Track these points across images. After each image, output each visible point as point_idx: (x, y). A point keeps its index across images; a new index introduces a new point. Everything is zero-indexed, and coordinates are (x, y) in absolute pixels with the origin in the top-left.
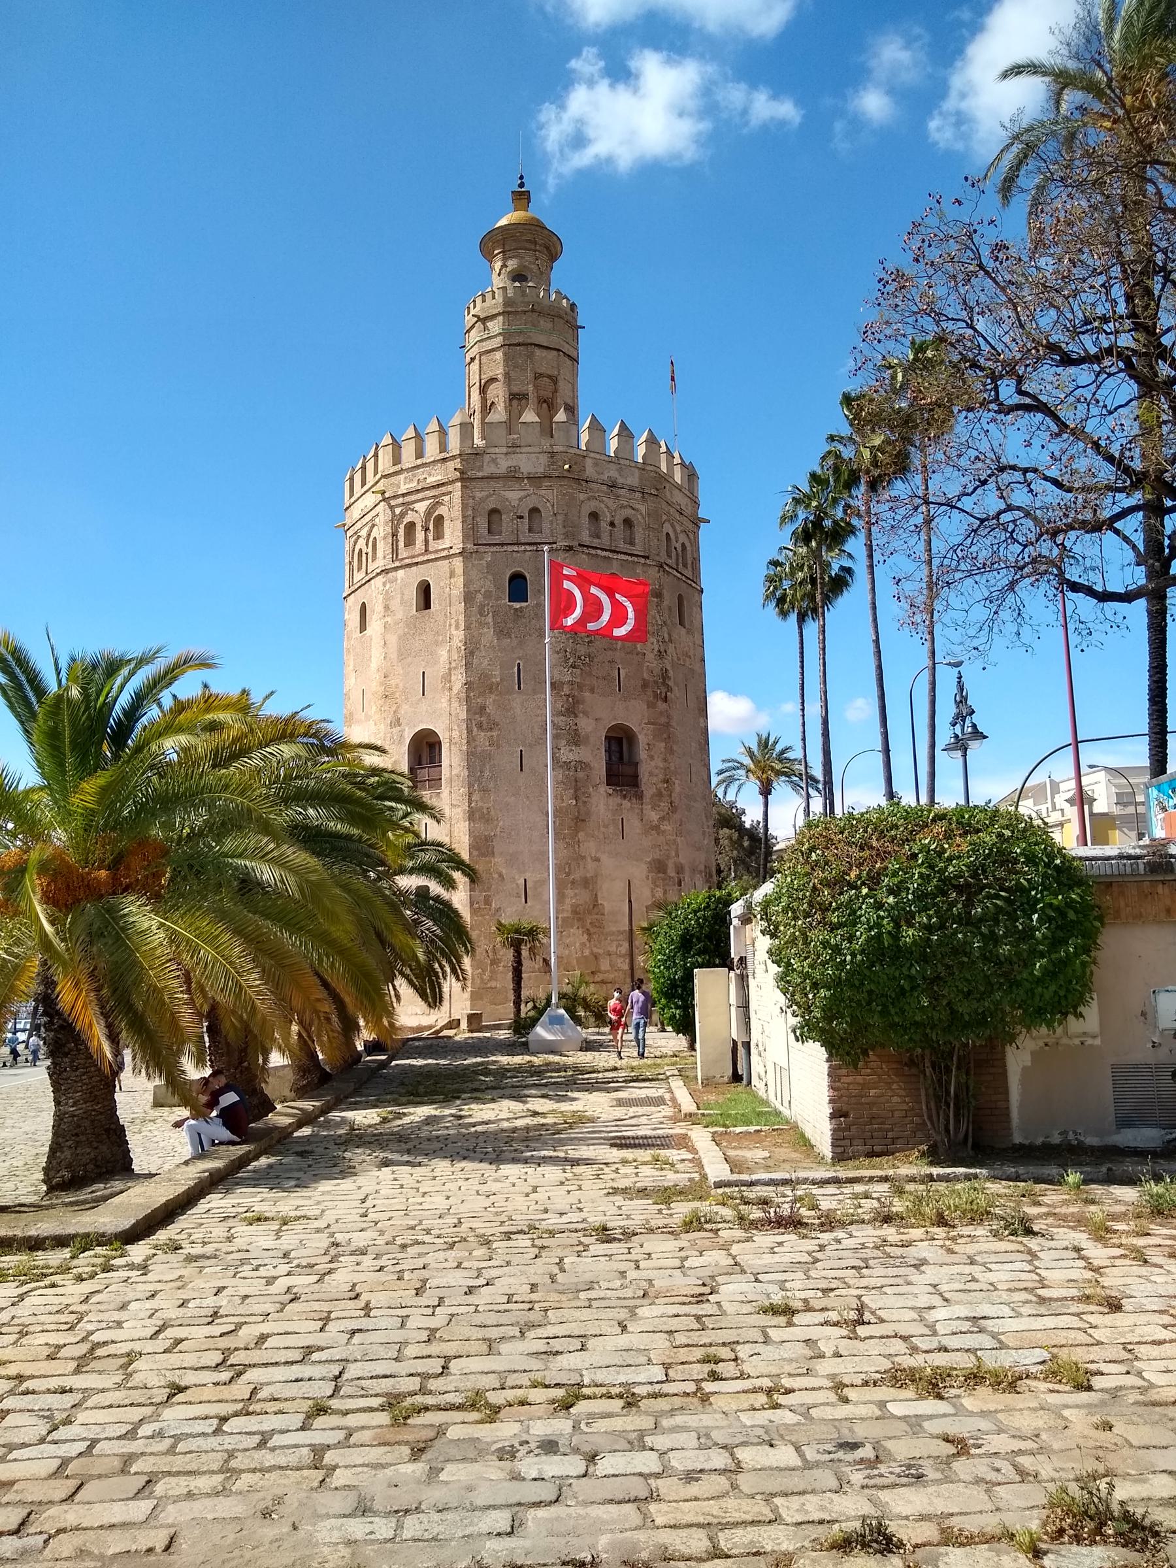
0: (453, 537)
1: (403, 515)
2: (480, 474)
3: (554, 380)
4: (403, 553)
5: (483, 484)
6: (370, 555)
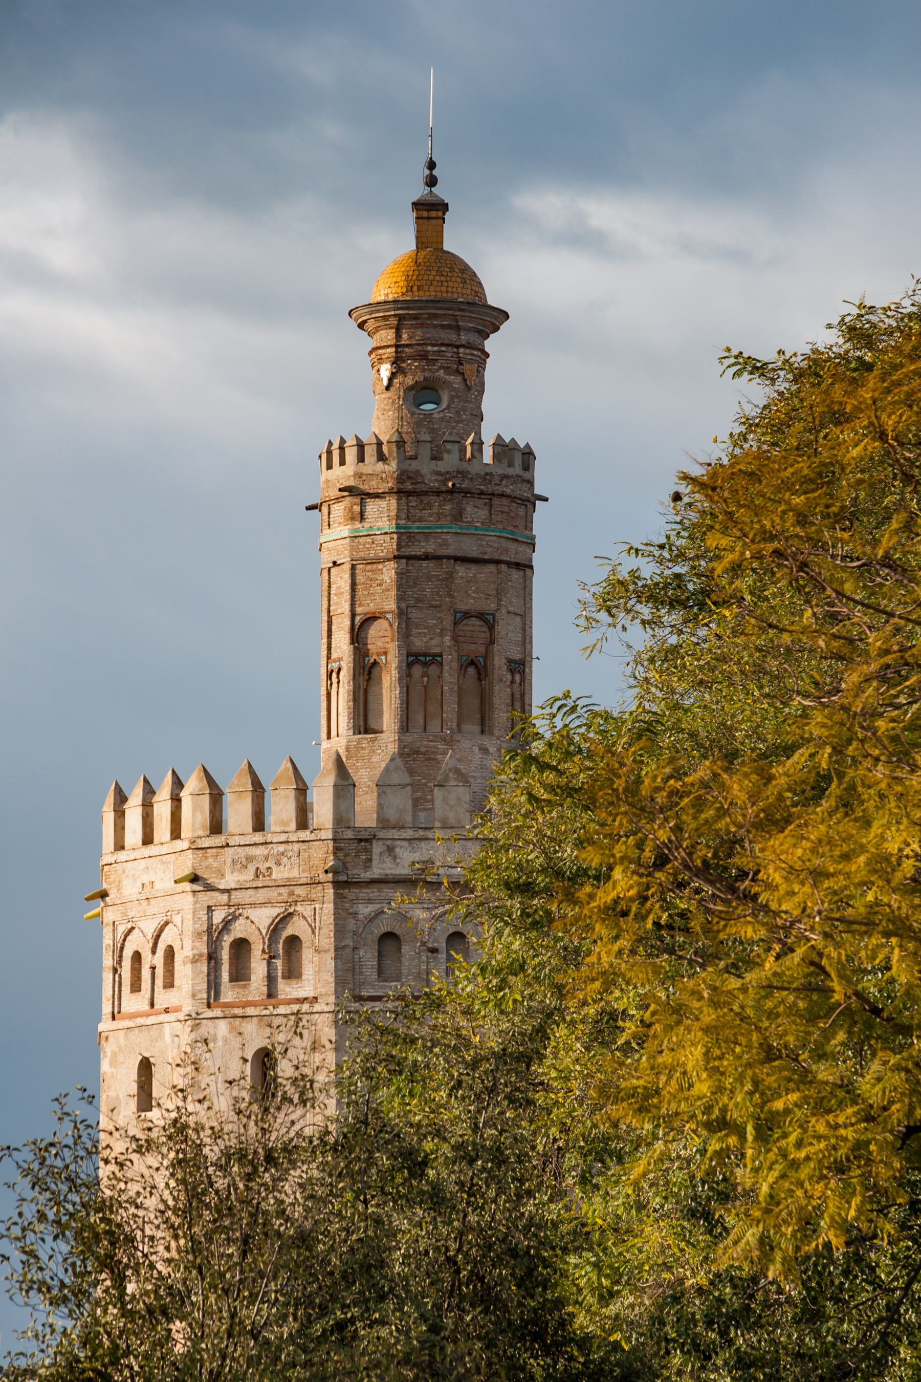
0: (317, 977)
1: (227, 924)
2: (367, 875)
3: (488, 620)
4: (229, 994)
5: (372, 892)
6: (160, 972)
